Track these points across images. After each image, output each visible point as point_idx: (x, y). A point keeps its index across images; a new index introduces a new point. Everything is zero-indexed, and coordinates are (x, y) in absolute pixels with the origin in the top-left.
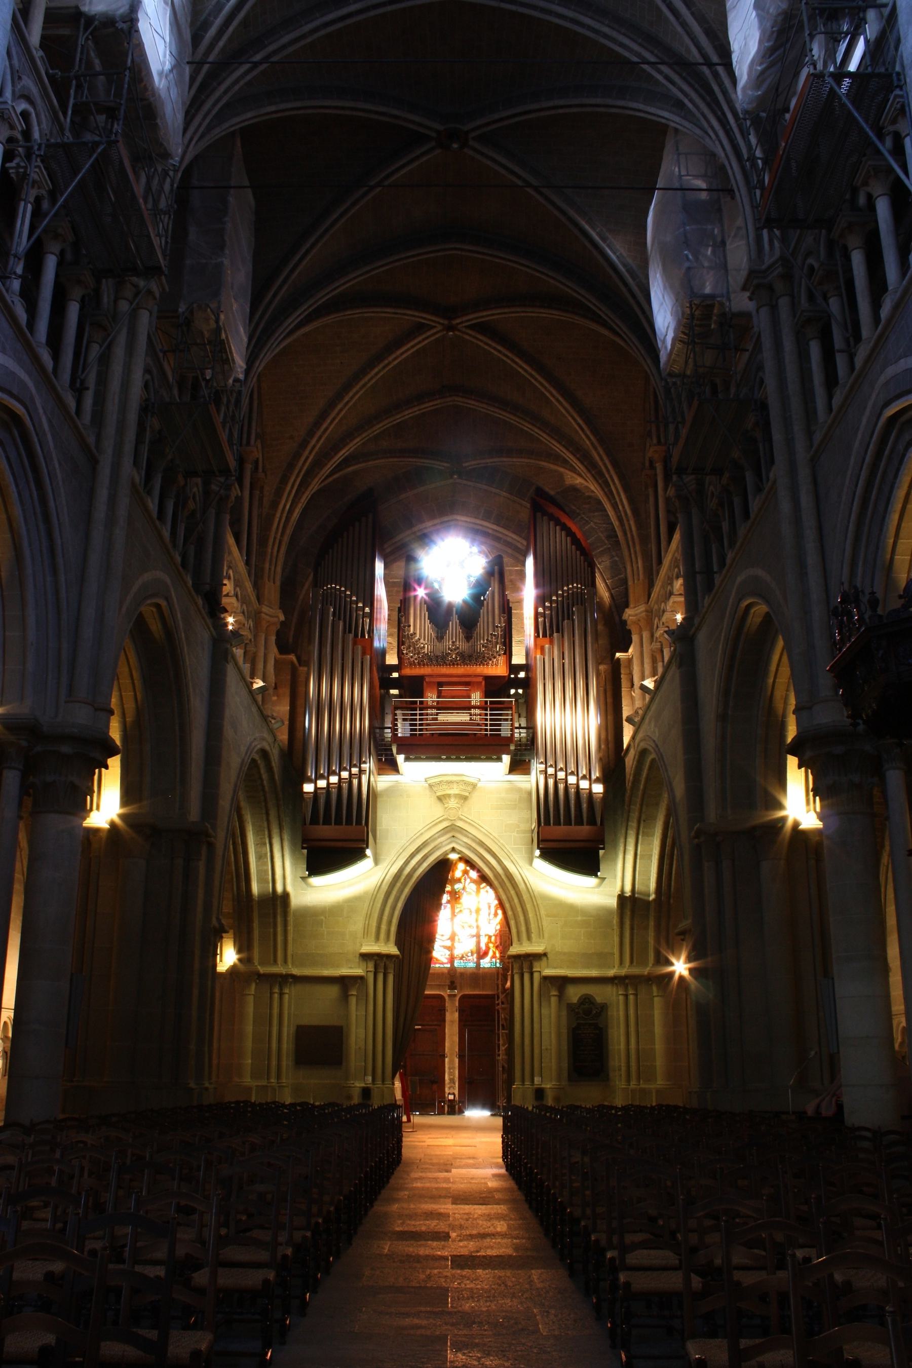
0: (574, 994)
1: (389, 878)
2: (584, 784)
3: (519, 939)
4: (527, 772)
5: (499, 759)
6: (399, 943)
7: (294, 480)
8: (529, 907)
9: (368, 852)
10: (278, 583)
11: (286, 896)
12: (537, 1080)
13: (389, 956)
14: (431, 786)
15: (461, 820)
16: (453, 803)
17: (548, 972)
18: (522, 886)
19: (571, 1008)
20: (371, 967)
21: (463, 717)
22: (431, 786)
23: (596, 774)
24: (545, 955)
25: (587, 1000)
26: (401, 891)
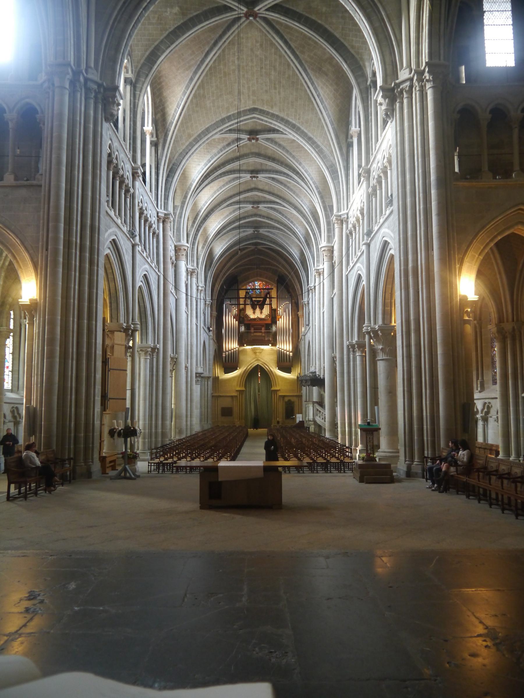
0: (286, 399)
2: (288, 353)
4: (276, 346)
6: (245, 387)
7: (219, 280)
8: (276, 378)
11: (218, 377)
12: (278, 419)
13: (243, 391)
16: (258, 354)
17: (280, 394)
18: (274, 374)
20: (239, 393)
23: (291, 350)
24: (280, 390)
25: (289, 401)
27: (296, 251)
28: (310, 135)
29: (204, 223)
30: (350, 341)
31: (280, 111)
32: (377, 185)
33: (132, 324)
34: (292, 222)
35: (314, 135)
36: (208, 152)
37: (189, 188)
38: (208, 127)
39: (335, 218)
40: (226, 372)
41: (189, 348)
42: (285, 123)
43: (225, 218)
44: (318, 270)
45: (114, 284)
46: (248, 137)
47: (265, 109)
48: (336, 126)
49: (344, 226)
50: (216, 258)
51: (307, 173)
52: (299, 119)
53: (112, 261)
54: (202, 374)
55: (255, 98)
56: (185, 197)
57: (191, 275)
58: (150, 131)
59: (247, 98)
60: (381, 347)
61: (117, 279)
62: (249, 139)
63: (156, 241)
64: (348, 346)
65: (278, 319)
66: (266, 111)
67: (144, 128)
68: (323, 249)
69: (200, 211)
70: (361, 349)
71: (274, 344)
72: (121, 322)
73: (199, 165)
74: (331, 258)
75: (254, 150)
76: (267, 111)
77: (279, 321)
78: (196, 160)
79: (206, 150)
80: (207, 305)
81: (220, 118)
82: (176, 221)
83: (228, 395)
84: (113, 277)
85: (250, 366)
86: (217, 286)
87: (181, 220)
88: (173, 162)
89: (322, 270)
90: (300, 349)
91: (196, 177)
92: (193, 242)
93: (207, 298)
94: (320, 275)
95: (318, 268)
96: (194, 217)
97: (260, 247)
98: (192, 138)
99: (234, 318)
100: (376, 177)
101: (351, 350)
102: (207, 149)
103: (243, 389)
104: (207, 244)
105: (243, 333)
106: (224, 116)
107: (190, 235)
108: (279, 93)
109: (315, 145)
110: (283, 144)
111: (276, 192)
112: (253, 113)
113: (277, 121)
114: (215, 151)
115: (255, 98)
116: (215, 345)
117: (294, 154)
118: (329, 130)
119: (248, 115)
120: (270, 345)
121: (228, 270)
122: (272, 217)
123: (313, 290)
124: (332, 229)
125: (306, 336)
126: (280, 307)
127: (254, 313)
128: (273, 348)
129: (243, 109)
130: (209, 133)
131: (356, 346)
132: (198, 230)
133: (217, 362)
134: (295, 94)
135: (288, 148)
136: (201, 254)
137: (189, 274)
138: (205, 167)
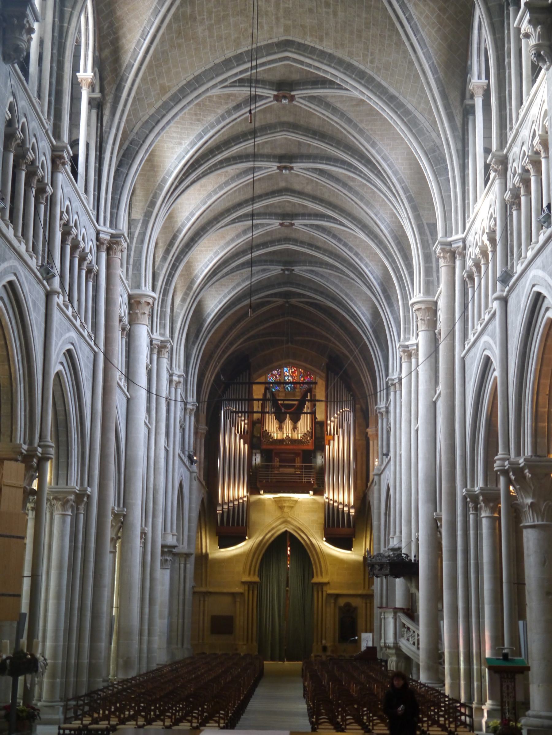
0: (342, 602)
1: (255, 545)
2: (346, 509)
3: (317, 575)
5: (308, 493)
6: (260, 576)
7: (212, 363)
8: (322, 560)
9: (247, 538)
10: (205, 413)
11: (207, 554)
13: (255, 583)
14: (275, 501)
15: (290, 517)
16: (286, 510)
18: (318, 550)
19: (340, 608)
20: (247, 588)
21: (292, 470)
22: (275, 501)
24: (328, 583)
25: (348, 605)
26: (262, 550)
27: (364, 309)
28: (392, 91)
29: (187, 253)
30: (468, 487)
31: (337, 47)
32: (521, 185)
33: (39, 446)
34: (356, 254)
35: (399, 93)
36: (199, 120)
37: (161, 188)
38: (199, 75)
39: (439, 247)
40: (223, 544)
41: (151, 496)
42: (345, 69)
43: (228, 243)
44: (407, 347)
45: (7, 367)
46: (276, 93)
47: (306, 43)
48: (441, 75)
49: (458, 263)
50: (209, 320)
51: (386, 162)
52: (372, 62)
53: (6, 323)
54: (174, 547)
55: (290, 22)
56: (152, 204)
57: (159, 352)
58: (90, 80)
59: (274, 22)
60: (529, 501)
61: (13, 357)
62: (277, 98)
63: (93, 286)
64: (465, 498)
65: (327, 442)
66: (309, 46)
67: (78, 74)
68: (416, 307)
69: (179, 231)
70: (491, 505)
71: (319, 491)
72: (18, 442)
73: (180, 144)
74: (433, 323)
75: (285, 119)
76: (312, 47)
77: (329, 445)
78: (175, 135)
79: (193, 117)
80: (188, 411)
81: (223, 58)
82: (133, 249)
83: (225, 590)
84: (5, 353)
85: (269, 535)
86: (208, 375)
87: (142, 247)
88: (130, 138)
89: (415, 347)
90: (371, 501)
91: (173, 166)
92: (165, 289)
93: (190, 399)
94: (410, 356)
95: (407, 343)
96: (168, 243)
97: (293, 301)
98: (169, 95)
99: (240, 439)
100: (519, 171)
101: (471, 505)
102: (196, 114)
103: (256, 579)
104: (191, 294)
105: (257, 467)
106: (230, 54)
107: (159, 274)
108: (335, 14)
109: (402, 110)
110: (341, 107)
111: (326, 196)
112: (286, 51)
113: (329, 66)
114: (211, 118)
115: (290, 22)
116: (203, 491)
117: (361, 126)
118: (428, 83)
119: (275, 53)
120: (311, 492)
121: (231, 344)
122: (319, 244)
123: (397, 385)
124: (435, 269)
125: (382, 476)
126: (332, 419)
127: (281, 428)
128: (317, 498)
129: (265, 43)
130: (200, 86)
131: (481, 498)
132: (174, 267)
133: (206, 525)
134: (364, 15)
135: (351, 116)
136: (180, 313)
137: (156, 351)
138: (192, 148)
